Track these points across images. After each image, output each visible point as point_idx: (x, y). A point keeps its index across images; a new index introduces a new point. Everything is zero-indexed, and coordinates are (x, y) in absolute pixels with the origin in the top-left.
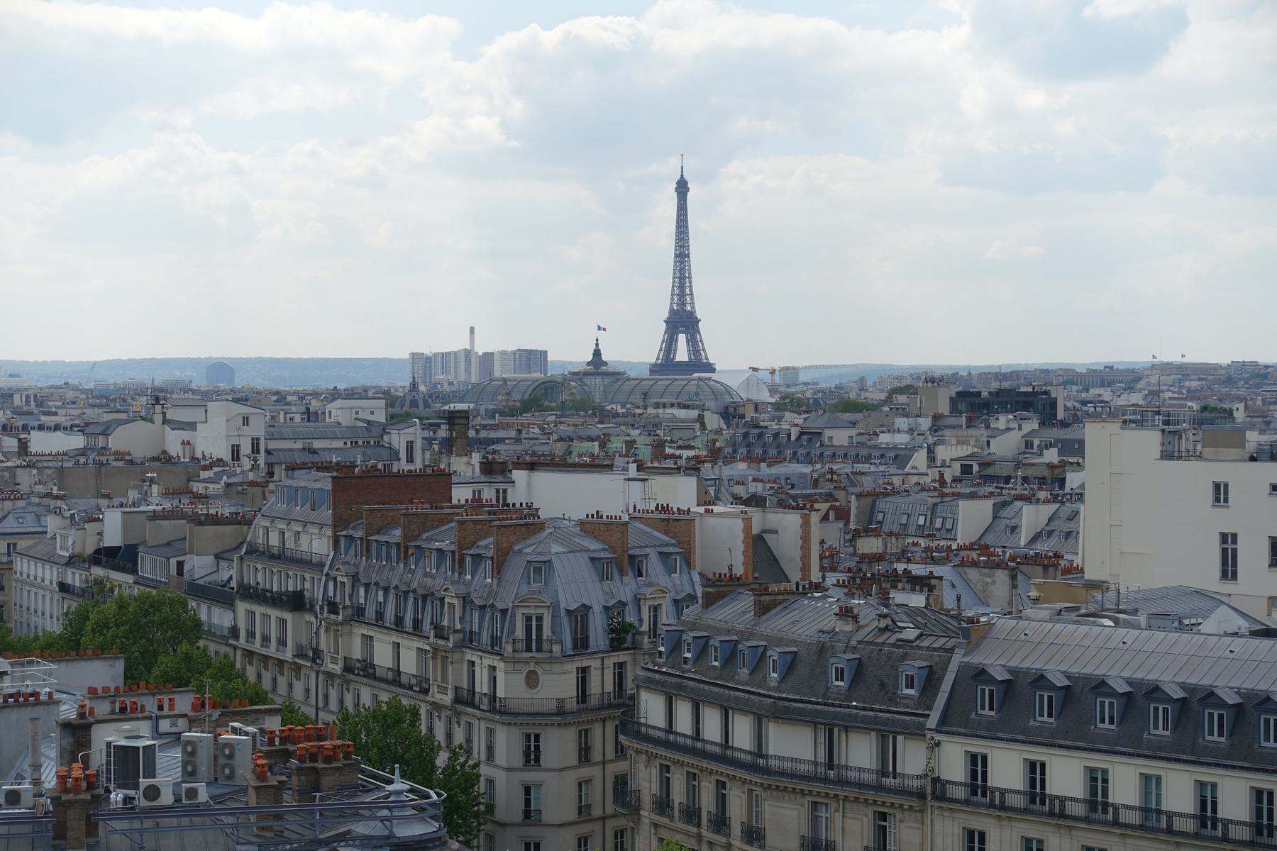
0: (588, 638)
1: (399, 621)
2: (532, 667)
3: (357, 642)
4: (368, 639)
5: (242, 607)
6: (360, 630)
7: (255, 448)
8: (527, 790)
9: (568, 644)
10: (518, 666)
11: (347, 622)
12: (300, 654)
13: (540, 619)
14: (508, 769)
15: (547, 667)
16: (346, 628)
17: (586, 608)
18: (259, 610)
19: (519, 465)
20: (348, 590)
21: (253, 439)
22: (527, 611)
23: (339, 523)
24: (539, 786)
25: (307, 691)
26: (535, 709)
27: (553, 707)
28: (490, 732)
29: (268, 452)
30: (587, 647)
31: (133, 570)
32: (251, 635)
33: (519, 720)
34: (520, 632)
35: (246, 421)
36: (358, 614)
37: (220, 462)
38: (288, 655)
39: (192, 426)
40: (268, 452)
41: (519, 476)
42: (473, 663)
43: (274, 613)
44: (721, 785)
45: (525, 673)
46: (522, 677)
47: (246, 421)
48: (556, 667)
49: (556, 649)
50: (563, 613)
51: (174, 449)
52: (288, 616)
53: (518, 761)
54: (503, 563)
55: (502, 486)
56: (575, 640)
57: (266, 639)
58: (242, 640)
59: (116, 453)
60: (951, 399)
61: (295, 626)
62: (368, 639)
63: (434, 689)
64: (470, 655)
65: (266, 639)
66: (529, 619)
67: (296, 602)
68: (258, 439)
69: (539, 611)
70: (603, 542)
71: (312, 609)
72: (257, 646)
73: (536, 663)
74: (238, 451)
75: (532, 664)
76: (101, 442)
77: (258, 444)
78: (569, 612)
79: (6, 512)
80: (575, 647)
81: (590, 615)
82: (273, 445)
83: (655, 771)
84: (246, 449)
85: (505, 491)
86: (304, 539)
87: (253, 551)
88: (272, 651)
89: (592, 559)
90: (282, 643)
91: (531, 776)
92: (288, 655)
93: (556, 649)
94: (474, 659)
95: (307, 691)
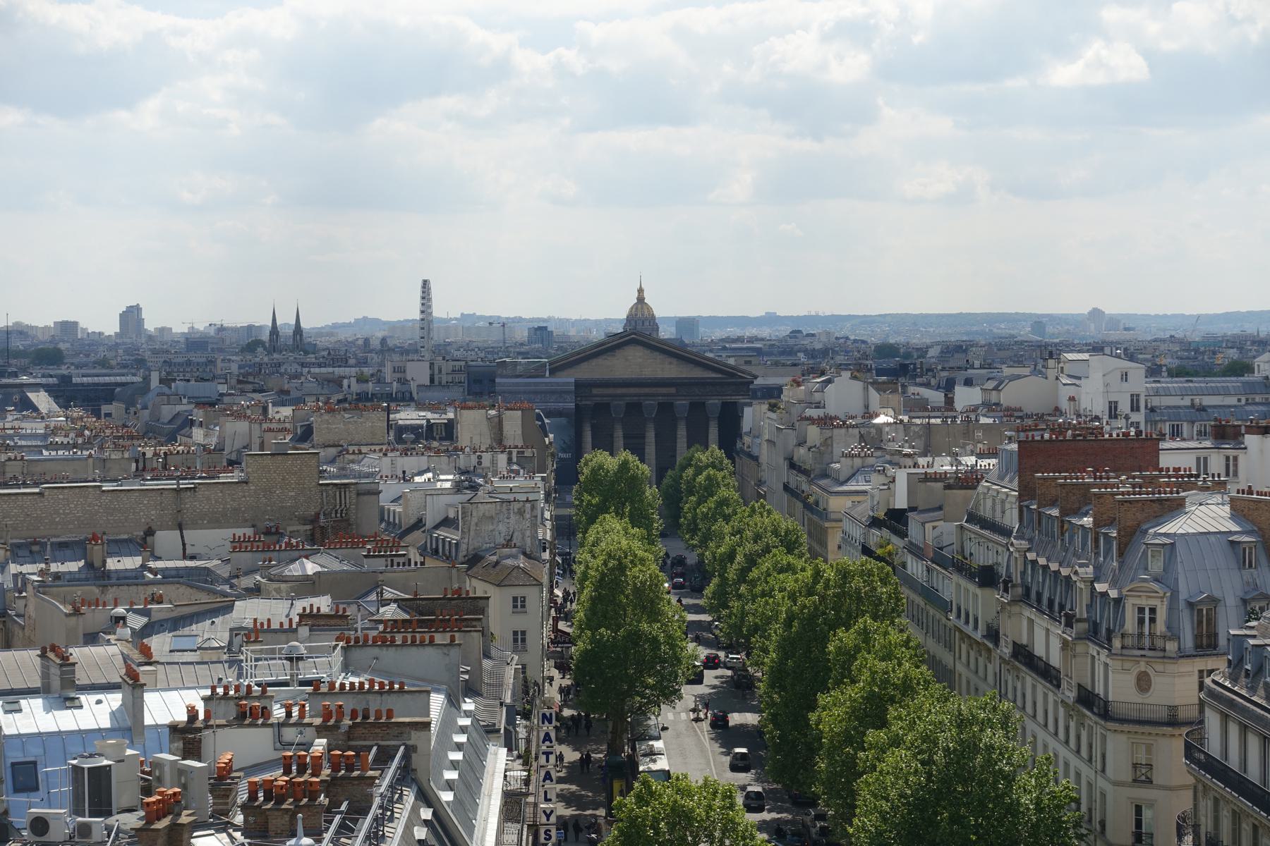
0: (1216, 635)
1: (1051, 603)
2: (1142, 666)
3: (1025, 623)
4: (1031, 622)
6: (1028, 613)
7: (1135, 407)
8: (1138, 810)
9: (1188, 642)
10: (1127, 665)
11: (1013, 602)
13: (1153, 611)
14: (1116, 784)
15: (1159, 667)
16: (1015, 609)
17: (1214, 601)
19: (1250, 430)
21: (1132, 395)
22: (1138, 602)
23: (1026, 492)
24: (1151, 805)
26: (1146, 715)
27: (1163, 714)
28: (1104, 738)
30: (1215, 646)
31: (903, 535)
33: (1126, 727)
34: (1130, 625)
35: (1125, 377)
36: (1025, 598)
38: (978, 636)
41: (1251, 440)
42: (1093, 657)
44: (1255, 828)
45: (1135, 673)
46: (1130, 679)
47: (1125, 377)
48: (1171, 668)
49: (1171, 647)
50: (1182, 605)
51: (1064, 405)
52: (979, 591)
53: (1127, 776)
54: (1126, 545)
55: (1232, 453)
56: (1197, 637)
59: (1008, 409)
62: (1031, 622)
63: (1064, 684)
64: (1093, 649)
66: (1141, 610)
67: (987, 577)
68: (1138, 395)
69: (1152, 602)
70: (1253, 523)
73: (1147, 663)
74: (1116, 408)
75: (1142, 664)
76: (994, 397)
77: (1138, 401)
78: (1191, 605)
79: (855, 468)
80: (1198, 646)
81: (1221, 610)
82: (1156, 401)
83: (1210, 803)
84: (1124, 407)
85: (1236, 458)
89: (1232, 542)
91: (1142, 793)
92: (978, 636)
93: (1171, 647)
94: (1095, 654)
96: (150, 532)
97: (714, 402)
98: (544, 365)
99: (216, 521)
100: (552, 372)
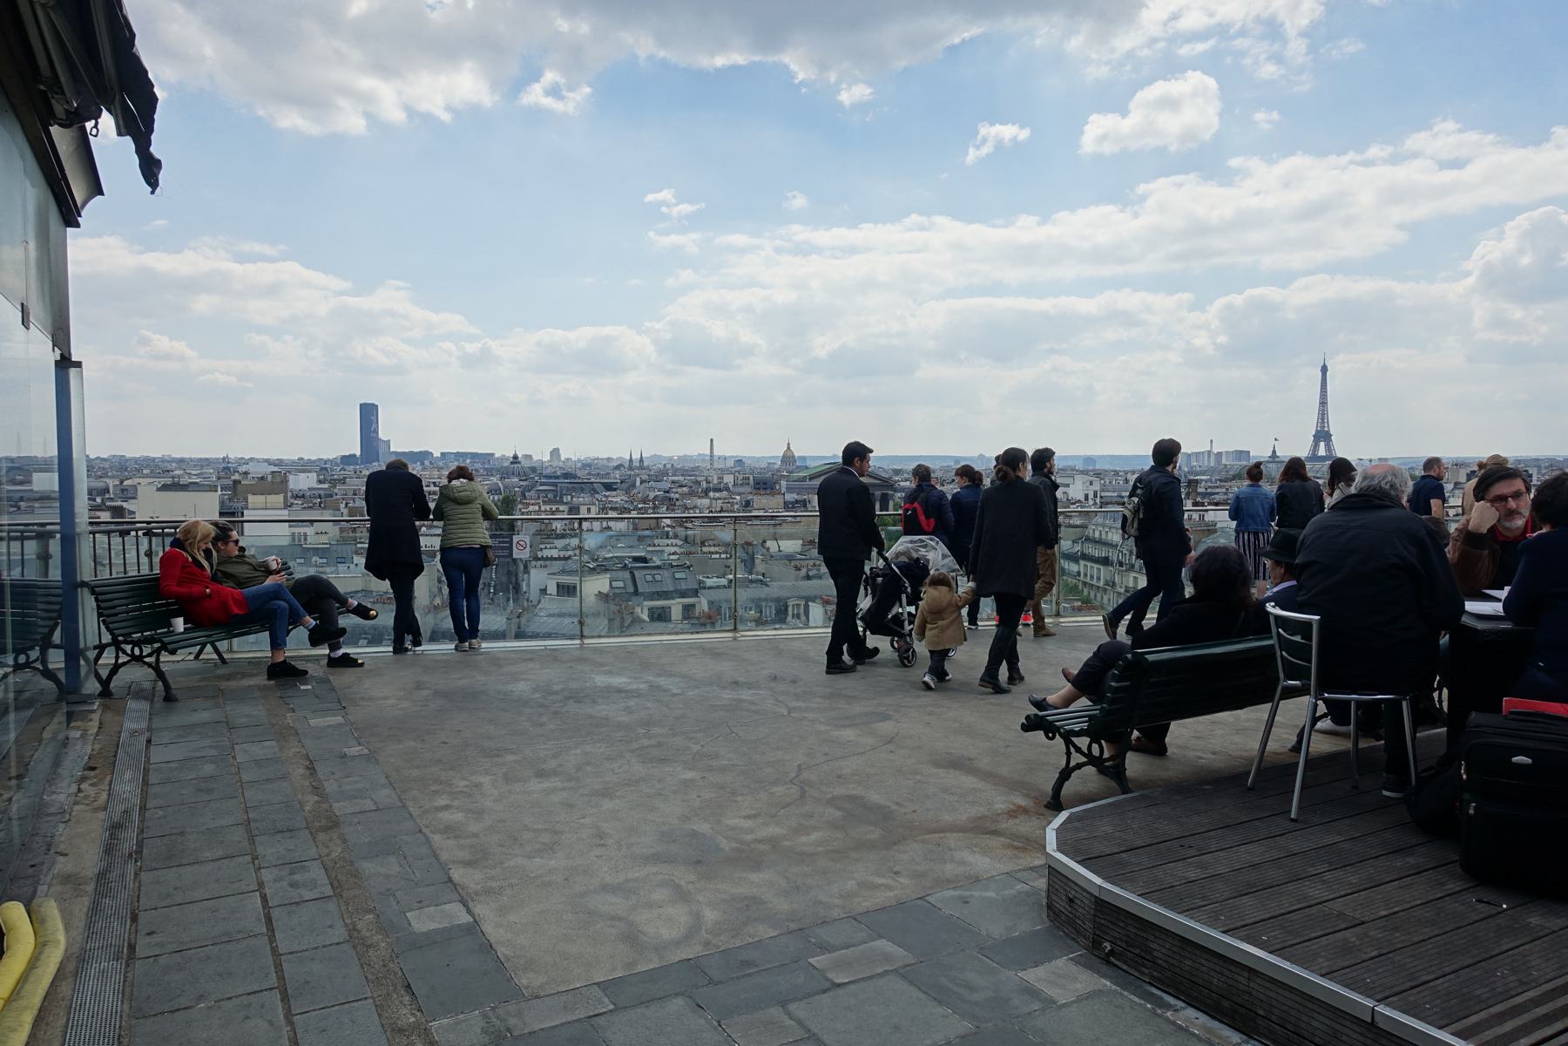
3: (1131, 580)
5: (1082, 563)
6: (1134, 574)
7: (1095, 496)
11: (1126, 571)
12: (1107, 583)
16: (1127, 573)
18: (1089, 564)
20: (1128, 557)
25: (1109, 600)
29: (1101, 497)
32: (1086, 575)
35: (1091, 483)
37: (1079, 501)
38: (1101, 584)
39: (1068, 486)
40: (1101, 497)
43: (1096, 566)
47: (1091, 483)
52: (1102, 567)
57: (1092, 577)
58: (1082, 577)
60: (1467, 474)
61: (1105, 572)
65: (1092, 577)
67: (1105, 561)
71: (1112, 565)
72: (1088, 580)
82: (1103, 494)
84: (1091, 496)
86: (1110, 534)
87: (1088, 539)
88: (1094, 582)
90: (1099, 579)
92: (1101, 584)
95: (1109, 600)
96: (764, 542)
97: (878, 493)
98: (806, 477)
99: (790, 537)
100: (810, 479)
